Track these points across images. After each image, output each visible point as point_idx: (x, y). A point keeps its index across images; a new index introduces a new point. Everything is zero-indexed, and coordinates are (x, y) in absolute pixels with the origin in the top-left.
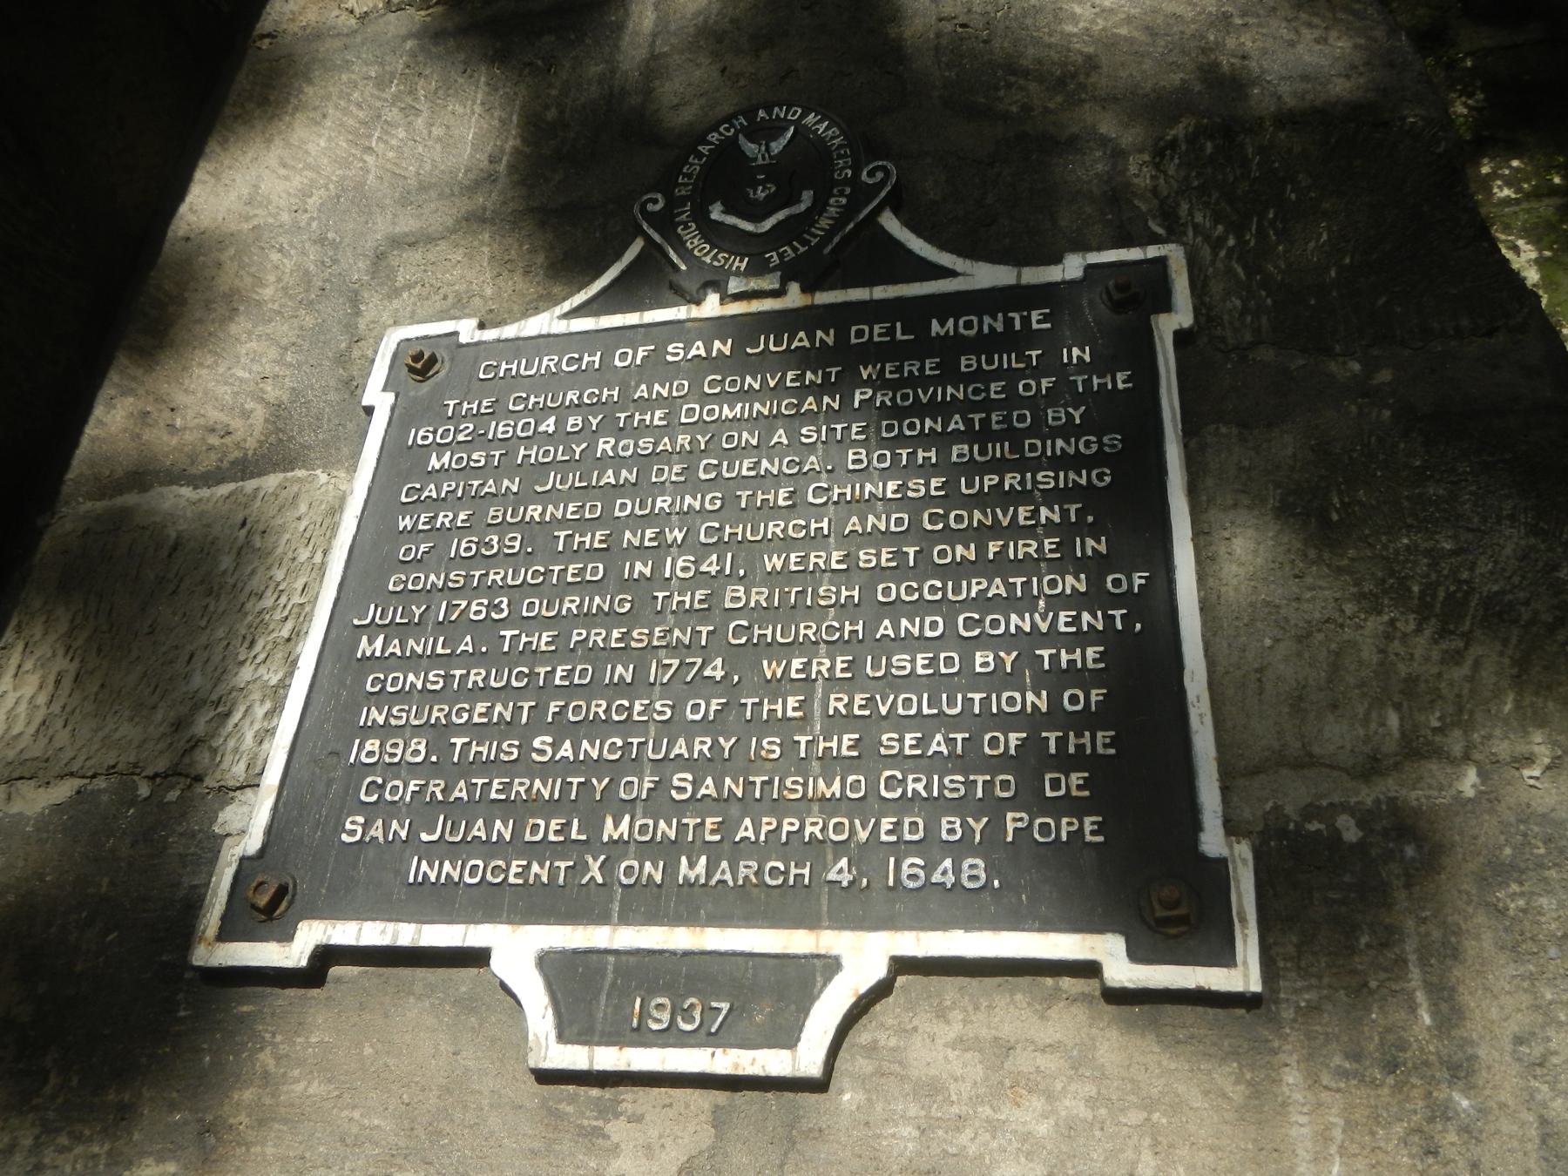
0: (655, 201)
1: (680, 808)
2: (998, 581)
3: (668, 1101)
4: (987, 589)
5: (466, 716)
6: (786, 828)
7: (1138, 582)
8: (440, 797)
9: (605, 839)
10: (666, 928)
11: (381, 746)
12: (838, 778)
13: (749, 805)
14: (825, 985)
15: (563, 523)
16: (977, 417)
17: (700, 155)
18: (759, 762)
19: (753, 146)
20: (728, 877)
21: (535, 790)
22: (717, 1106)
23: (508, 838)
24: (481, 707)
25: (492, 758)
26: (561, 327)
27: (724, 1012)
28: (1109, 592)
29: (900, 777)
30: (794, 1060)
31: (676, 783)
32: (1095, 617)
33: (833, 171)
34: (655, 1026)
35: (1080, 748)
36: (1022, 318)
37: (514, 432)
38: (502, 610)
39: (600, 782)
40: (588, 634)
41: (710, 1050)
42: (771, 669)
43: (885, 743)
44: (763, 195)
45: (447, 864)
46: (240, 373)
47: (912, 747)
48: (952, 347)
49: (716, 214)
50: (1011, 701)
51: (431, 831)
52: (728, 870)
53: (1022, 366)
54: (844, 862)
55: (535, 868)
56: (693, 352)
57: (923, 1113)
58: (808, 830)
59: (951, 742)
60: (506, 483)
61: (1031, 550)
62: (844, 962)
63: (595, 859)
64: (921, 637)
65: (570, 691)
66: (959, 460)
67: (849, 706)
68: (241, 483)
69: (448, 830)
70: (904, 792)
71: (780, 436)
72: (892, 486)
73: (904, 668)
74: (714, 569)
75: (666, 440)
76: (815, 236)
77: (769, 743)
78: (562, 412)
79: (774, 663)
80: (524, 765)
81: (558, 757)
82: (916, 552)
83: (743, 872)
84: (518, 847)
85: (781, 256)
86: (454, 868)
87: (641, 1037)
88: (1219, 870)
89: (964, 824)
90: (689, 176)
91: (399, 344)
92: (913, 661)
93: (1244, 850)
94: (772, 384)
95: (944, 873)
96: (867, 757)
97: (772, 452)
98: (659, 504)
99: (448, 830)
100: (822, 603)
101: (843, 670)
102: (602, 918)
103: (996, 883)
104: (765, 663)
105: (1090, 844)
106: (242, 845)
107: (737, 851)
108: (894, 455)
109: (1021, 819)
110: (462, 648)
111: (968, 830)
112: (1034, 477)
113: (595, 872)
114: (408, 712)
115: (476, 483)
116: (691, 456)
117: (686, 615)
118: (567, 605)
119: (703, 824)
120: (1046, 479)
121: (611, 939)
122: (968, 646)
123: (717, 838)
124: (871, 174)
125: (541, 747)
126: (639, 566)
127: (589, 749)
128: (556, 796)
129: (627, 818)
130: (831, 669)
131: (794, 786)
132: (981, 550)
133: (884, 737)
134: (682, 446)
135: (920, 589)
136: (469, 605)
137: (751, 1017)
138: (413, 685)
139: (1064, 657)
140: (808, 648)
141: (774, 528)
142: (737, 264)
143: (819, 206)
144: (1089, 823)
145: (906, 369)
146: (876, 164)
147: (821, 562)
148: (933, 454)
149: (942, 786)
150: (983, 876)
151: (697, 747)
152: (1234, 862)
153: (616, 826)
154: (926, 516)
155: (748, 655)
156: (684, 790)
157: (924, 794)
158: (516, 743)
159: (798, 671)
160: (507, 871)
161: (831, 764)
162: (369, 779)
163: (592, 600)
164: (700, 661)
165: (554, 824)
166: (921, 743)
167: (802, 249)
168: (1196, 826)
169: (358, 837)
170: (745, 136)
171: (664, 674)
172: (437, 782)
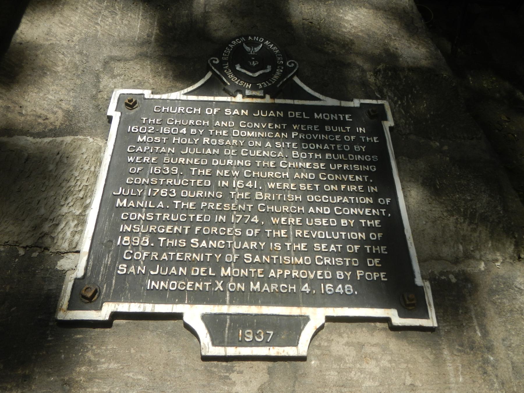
0: (216, 60)
1: (248, 266)
2: (345, 197)
3: (251, 366)
5: (163, 230)
6: (286, 273)
7: (388, 201)
8: (157, 259)
9: (222, 275)
10: (248, 306)
11: (130, 239)
12: (301, 257)
13: (271, 265)
14: (305, 325)
15: (193, 165)
16: (333, 146)
17: (230, 48)
19: (248, 48)
20: (268, 289)
21: (193, 257)
22: (269, 367)
23: (185, 274)
24: (169, 227)
25: (176, 245)
26: (185, 98)
27: (272, 335)
29: (322, 258)
30: (298, 350)
31: (246, 257)
33: (277, 61)
34: (247, 340)
35: (377, 251)
36: (343, 116)
38: (173, 194)
39: (218, 255)
40: (208, 205)
41: (268, 348)
42: (274, 221)
43: (316, 247)
44: (255, 64)
46: (50, 97)
47: (324, 248)
48: (322, 123)
49: (238, 68)
50: (354, 235)
52: (267, 287)
53: (345, 131)
54: (306, 285)
55: (197, 285)
56: (234, 113)
57: (338, 367)
58: (293, 274)
59: (337, 248)
60: (169, 149)
61: (355, 189)
62: (311, 318)
63: (219, 282)
64: (323, 214)
65: (202, 224)
66: (329, 158)
67: (303, 234)
68: (54, 138)
69: (161, 270)
70: (324, 263)
71: (268, 144)
72: (308, 164)
74: (251, 186)
75: (228, 141)
76: (274, 81)
77: (277, 245)
78: (189, 127)
79: (275, 219)
80: (188, 248)
83: (272, 288)
84: (189, 277)
85: (262, 85)
86: (165, 284)
87: (243, 343)
88: (420, 290)
89: (344, 274)
90: (227, 54)
91: (120, 95)
92: (322, 221)
93: (427, 284)
94: (264, 127)
95: (340, 289)
96: (310, 251)
97: (266, 149)
98: (228, 162)
99: (161, 270)
100: (289, 200)
101: (299, 222)
102: (224, 303)
103: (356, 293)
104: (272, 218)
105: (383, 281)
106: (75, 274)
107: (270, 281)
108: (307, 154)
109: (361, 273)
110: (159, 206)
111: (346, 276)
113: (219, 286)
115: (157, 148)
116: (238, 147)
117: (242, 201)
119: (257, 271)
120: (356, 167)
122: (339, 218)
123: (262, 276)
124: (290, 63)
125: (194, 242)
126: (223, 183)
127: (212, 244)
128: (202, 260)
129: (229, 268)
130: (295, 222)
131: (287, 260)
132: (339, 187)
133: (315, 245)
134: (234, 143)
135: (321, 198)
136: (160, 191)
137: (280, 336)
138: (141, 218)
141: (270, 174)
142: (247, 85)
143: (273, 72)
144: (382, 274)
145: (308, 128)
146: (291, 61)
148: (320, 155)
149: (335, 261)
150: (352, 290)
151: (252, 245)
152: (425, 287)
153: (226, 271)
154: (320, 175)
155: (266, 216)
156: (249, 259)
157: (330, 264)
158: (185, 241)
159: (284, 222)
160: (186, 285)
161: (298, 253)
162: (127, 251)
163: (207, 193)
164: (249, 216)
165: (202, 270)
166: (328, 247)
167: (269, 84)
168: (413, 277)
169: (125, 272)
170: (245, 44)
171: (236, 220)
172: (155, 253)
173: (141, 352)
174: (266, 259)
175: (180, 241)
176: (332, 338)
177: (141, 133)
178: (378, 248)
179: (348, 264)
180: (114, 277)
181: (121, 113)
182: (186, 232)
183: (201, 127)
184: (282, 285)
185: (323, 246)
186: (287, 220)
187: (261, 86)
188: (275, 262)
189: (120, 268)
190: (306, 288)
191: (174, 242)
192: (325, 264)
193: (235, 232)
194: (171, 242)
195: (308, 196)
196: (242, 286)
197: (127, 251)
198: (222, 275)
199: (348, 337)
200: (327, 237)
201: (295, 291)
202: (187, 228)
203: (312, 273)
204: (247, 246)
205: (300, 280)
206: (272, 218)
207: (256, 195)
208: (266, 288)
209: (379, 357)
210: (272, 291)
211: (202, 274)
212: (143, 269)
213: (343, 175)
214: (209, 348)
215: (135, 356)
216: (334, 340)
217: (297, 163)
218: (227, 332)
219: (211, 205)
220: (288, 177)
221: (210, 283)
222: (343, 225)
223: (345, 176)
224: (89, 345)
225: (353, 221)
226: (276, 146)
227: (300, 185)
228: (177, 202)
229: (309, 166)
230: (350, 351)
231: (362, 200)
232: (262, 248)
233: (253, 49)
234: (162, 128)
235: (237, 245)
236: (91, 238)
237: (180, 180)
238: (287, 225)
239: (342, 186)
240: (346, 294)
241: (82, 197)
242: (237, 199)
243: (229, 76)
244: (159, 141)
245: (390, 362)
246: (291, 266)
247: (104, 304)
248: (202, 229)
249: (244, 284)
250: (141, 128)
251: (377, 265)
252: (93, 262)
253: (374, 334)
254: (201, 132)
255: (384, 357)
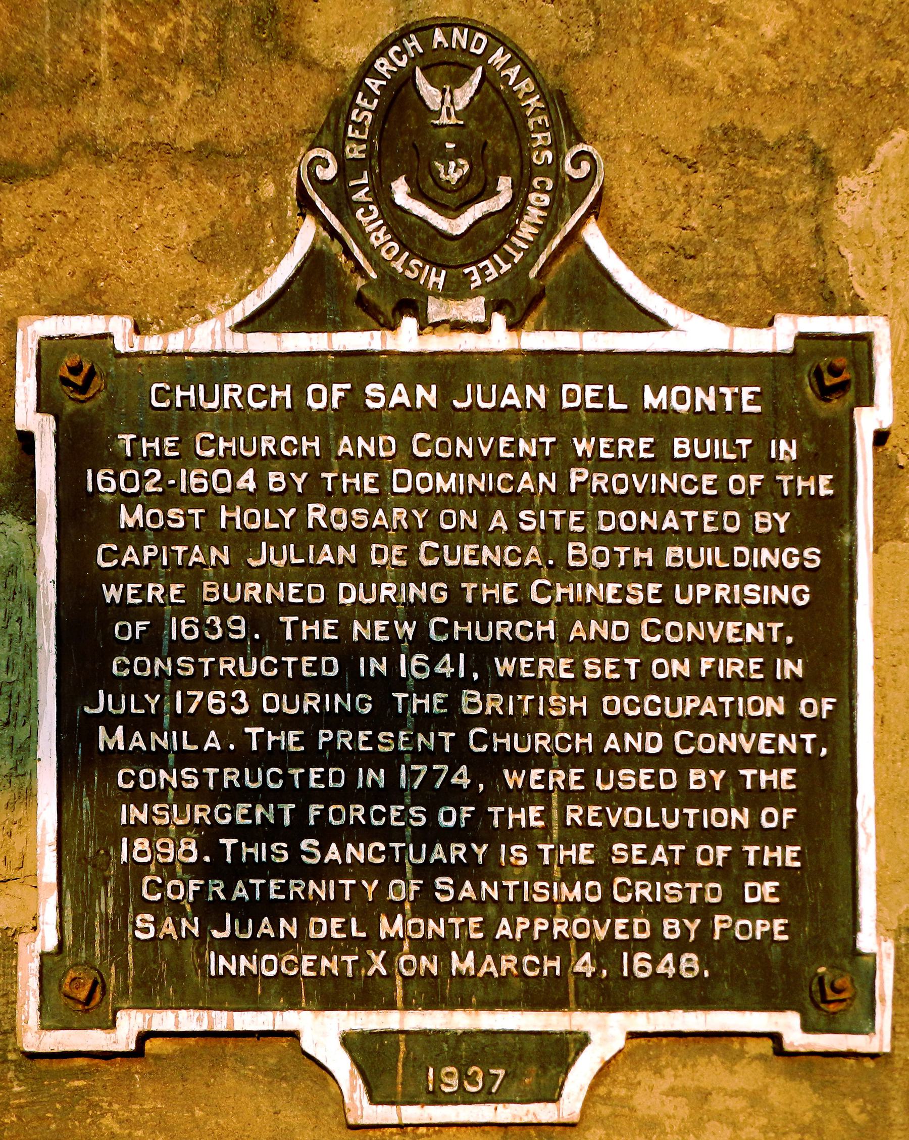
0: (326, 166)
1: (443, 910)
2: (709, 699)
4: (700, 708)
5: (228, 816)
6: (537, 928)
7: (827, 707)
8: (222, 897)
9: (383, 936)
11: (150, 846)
12: (578, 884)
13: (502, 906)
14: (577, 1054)
15: (286, 607)
16: (690, 514)
18: (509, 868)
20: (493, 969)
21: (310, 892)
23: (295, 935)
24: (242, 808)
25: (264, 859)
26: (238, 343)
27: (501, 1077)
28: (802, 716)
29: (629, 884)
30: (559, 1110)
31: (439, 886)
32: (790, 740)
33: (531, 150)
34: (447, 1090)
36: (734, 394)
37: (210, 485)
38: (241, 705)
39: (370, 884)
41: (494, 1105)
42: (513, 779)
43: (616, 853)
44: (457, 176)
45: (243, 958)
47: (638, 857)
49: (400, 191)
50: (719, 817)
51: (222, 929)
52: (492, 963)
53: (733, 457)
54: (587, 957)
55: (325, 962)
59: (670, 853)
61: (738, 669)
62: (593, 1037)
63: (377, 954)
64: (644, 753)
65: (327, 796)
66: (674, 565)
67: (584, 817)
69: (237, 928)
70: (634, 897)
71: (498, 521)
72: (612, 588)
73: (629, 782)
74: (449, 671)
75: (381, 512)
76: (518, 249)
77: (517, 850)
79: (515, 773)
81: (326, 860)
82: (637, 665)
83: (504, 965)
84: (303, 944)
85: (482, 272)
86: (251, 961)
87: (436, 1098)
89: (682, 924)
90: (359, 126)
91: (39, 343)
92: (637, 776)
93: (889, 947)
95: (667, 965)
97: (494, 539)
98: (384, 592)
99: (237, 928)
100: (554, 713)
101: (577, 782)
102: (390, 1005)
103: (706, 974)
104: (506, 772)
105: (777, 942)
108: (613, 552)
109: (726, 921)
111: (685, 931)
112: (742, 590)
113: (378, 964)
114: (170, 811)
117: (425, 722)
118: (307, 703)
119: (466, 923)
120: (754, 594)
121: (401, 1021)
122: (683, 765)
123: (481, 935)
124: (576, 164)
125: (309, 849)
128: (332, 897)
129: (399, 917)
130: (566, 781)
131: (540, 892)
132: (695, 666)
133: (615, 847)
135: (641, 704)
136: (205, 697)
137: (521, 1081)
139: (764, 777)
140: (543, 759)
141: (502, 628)
142: (433, 279)
143: (517, 206)
144: (778, 924)
145: (621, 447)
147: (549, 669)
148: (649, 555)
149: (664, 892)
150: (697, 968)
152: (881, 956)
153: (391, 925)
154: (644, 627)
156: (446, 893)
157: (650, 899)
158: (284, 845)
159: (537, 782)
160: (299, 965)
162: (147, 879)
164: (446, 768)
165: (336, 922)
166: (647, 853)
167: (506, 268)
168: (855, 927)
169: (151, 934)
170: (422, 70)
171: (414, 780)
172: (216, 882)
173: (217, 1114)
174: (490, 890)
175: (274, 847)
176: (639, 1077)
177: (125, 494)
178: (778, 854)
179: (693, 899)
180: (130, 948)
181: (57, 420)
182: (287, 821)
183: (296, 463)
184: (527, 959)
185: (637, 849)
186: (544, 779)
187: (476, 276)
188: (511, 898)
189: (139, 924)
190: (584, 964)
191: (258, 852)
192: (638, 900)
193: (410, 816)
194: (251, 850)
195: (606, 700)
196: (431, 962)
197: (147, 879)
198: (383, 936)
199: (676, 1076)
200: (649, 824)
201: (558, 973)
202: (288, 808)
203: (601, 926)
204: (442, 856)
205: (573, 944)
206: (506, 772)
207: (465, 701)
208: (489, 966)
209: (742, 1118)
210: (504, 974)
211: (335, 935)
212: (193, 925)
213: (710, 624)
214: (362, 1108)
215: (205, 1123)
216: (643, 1084)
217: (579, 586)
218: (400, 1071)
219: (343, 736)
220: (552, 637)
221: (356, 958)
222: (693, 786)
223: (716, 626)
224: (103, 1101)
225: (723, 772)
226: (524, 527)
227: (586, 662)
228: (254, 731)
229: (615, 596)
230: (676, 1108)
231: (757, 706)
232: (480, 860)
233: (448, 97)
234: (183, 472)
235: (417, 855)
236: (54, 847)
237: (254, 660)
238: (546, 792)
239: (703, 660)
240: (681, 977)
241: (4, 720)
242: (412, 715)
243: (372, 239)
244: (181, 525)
245: (764, 1130)
246: (549, 909)
247: (118, 1015)
248: (324, 812)
249: (435, 958)
250: (122, 476)
251: (768, 899)
252: (74, 909)
253: (736, 1068)
254: (299, 481)
255: (751, 1121)
